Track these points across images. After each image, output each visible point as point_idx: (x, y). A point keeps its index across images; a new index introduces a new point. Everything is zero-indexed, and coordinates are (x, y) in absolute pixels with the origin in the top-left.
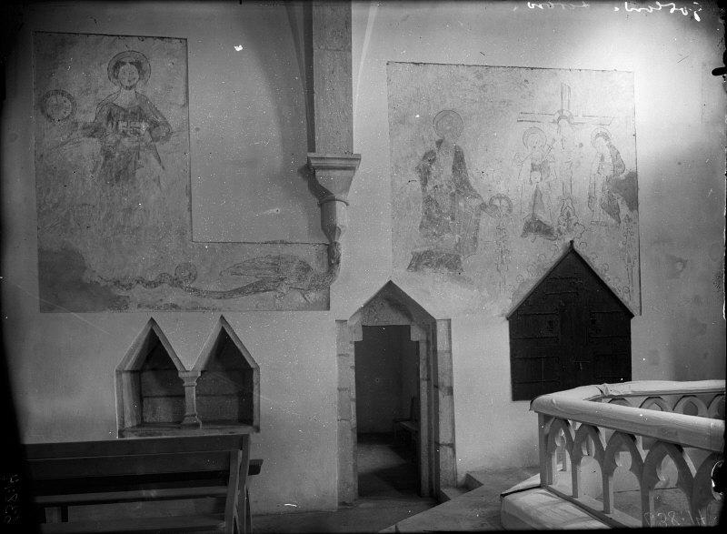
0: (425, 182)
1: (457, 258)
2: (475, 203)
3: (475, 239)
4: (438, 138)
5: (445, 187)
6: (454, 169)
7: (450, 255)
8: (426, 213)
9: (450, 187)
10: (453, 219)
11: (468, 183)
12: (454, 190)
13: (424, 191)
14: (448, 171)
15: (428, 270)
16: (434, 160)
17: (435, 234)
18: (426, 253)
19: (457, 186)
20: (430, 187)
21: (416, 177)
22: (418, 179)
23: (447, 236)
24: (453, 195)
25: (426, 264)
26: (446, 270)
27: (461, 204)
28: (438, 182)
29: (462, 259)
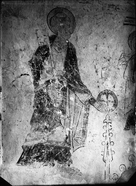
0: (37, 77)
1: (67, 150)
2: (84, 97)
3: (84, 132)
4: (51, 34)
5: (57, 82)
6: (66, 65)
7: (60, 148)
8: (37, 107)
9: (61, 82)
10: (64, 113)
11: (78, 79)
12: (65, 85)
13: (36, 85)
14: (60, 66)
15: (36, 163)
16: (47, 55)
17: (46, 128)
18: (36, 146)
19: (69, 81)
20: (42, 82)
21: (28, 70)
22: (30, 73)
23: (58, 129)
24: (64, 90)
25: (37, 158)
26: (56, 162)
27: (72, 98)
28: (50, 77)
29: (71, 151)
